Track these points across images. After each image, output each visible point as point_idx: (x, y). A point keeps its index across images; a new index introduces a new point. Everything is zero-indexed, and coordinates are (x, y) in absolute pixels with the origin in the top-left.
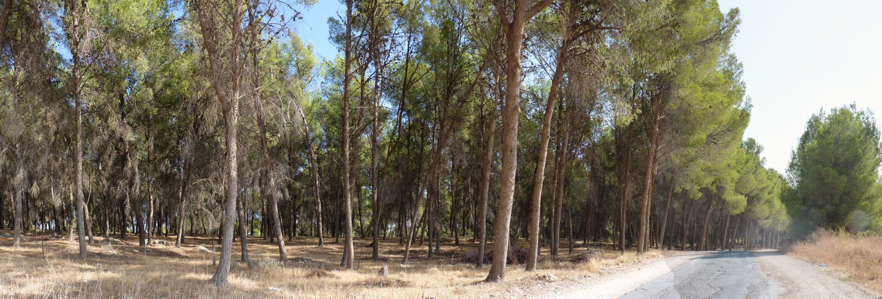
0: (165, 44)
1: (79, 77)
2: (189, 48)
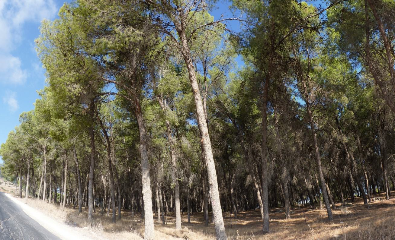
0: (355, 87)
1: (311, 113)
2: (369, 86)
